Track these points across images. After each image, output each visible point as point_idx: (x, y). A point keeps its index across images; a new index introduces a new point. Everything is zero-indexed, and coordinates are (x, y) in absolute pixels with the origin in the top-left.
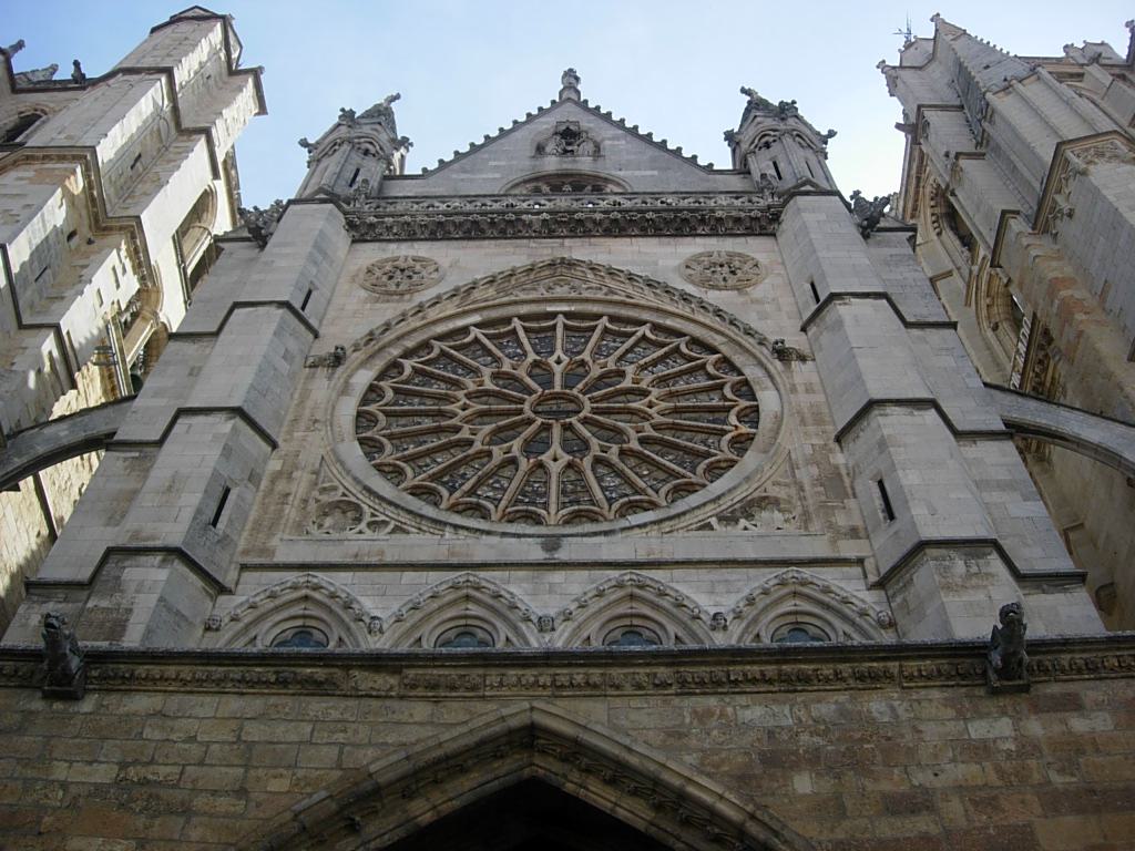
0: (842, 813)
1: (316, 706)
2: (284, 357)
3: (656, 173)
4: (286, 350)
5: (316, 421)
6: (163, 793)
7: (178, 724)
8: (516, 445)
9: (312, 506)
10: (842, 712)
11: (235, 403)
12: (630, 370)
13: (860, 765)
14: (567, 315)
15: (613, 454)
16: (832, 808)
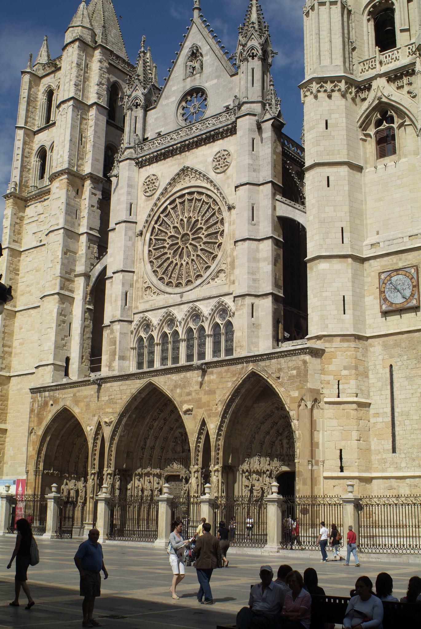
0: (181, 396)
1: (128, 382)
2: (129, 240)
3: (215, 81)
4: (129, 237)
5: (140, 259)
6: (114, 400)
7: (113, 388)
8: (177, 257)
9: (144, 289)
10: (184, 376)
11: (121, 268)
12: (200, 218)
13: (184, 387)
14: (189, 193)
15: (194, 258)
16: (180, 395)
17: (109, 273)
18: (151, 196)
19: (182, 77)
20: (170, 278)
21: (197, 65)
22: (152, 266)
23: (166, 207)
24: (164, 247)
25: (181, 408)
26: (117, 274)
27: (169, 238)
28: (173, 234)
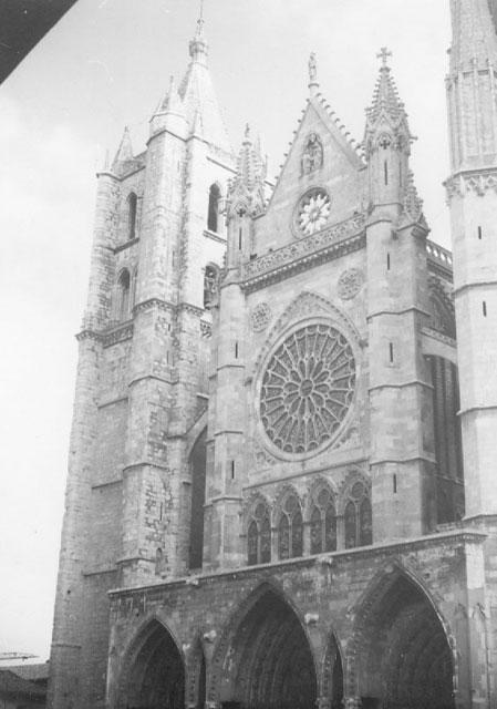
3: (338, 179)
8: (297, 412)
14: (309, 327)
15: (319, 413)
17: (210, 435)
18: (262, 330)
19: (298, 174)
20: (289, 440)
21: (316, 159)
22: (266, 426)
23: (282, 346)
24: (281, 399)
25: (303, 619)
26: (219, 437)
27: (286, 386)
28: (290, 381)
